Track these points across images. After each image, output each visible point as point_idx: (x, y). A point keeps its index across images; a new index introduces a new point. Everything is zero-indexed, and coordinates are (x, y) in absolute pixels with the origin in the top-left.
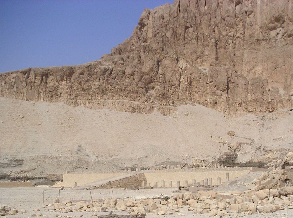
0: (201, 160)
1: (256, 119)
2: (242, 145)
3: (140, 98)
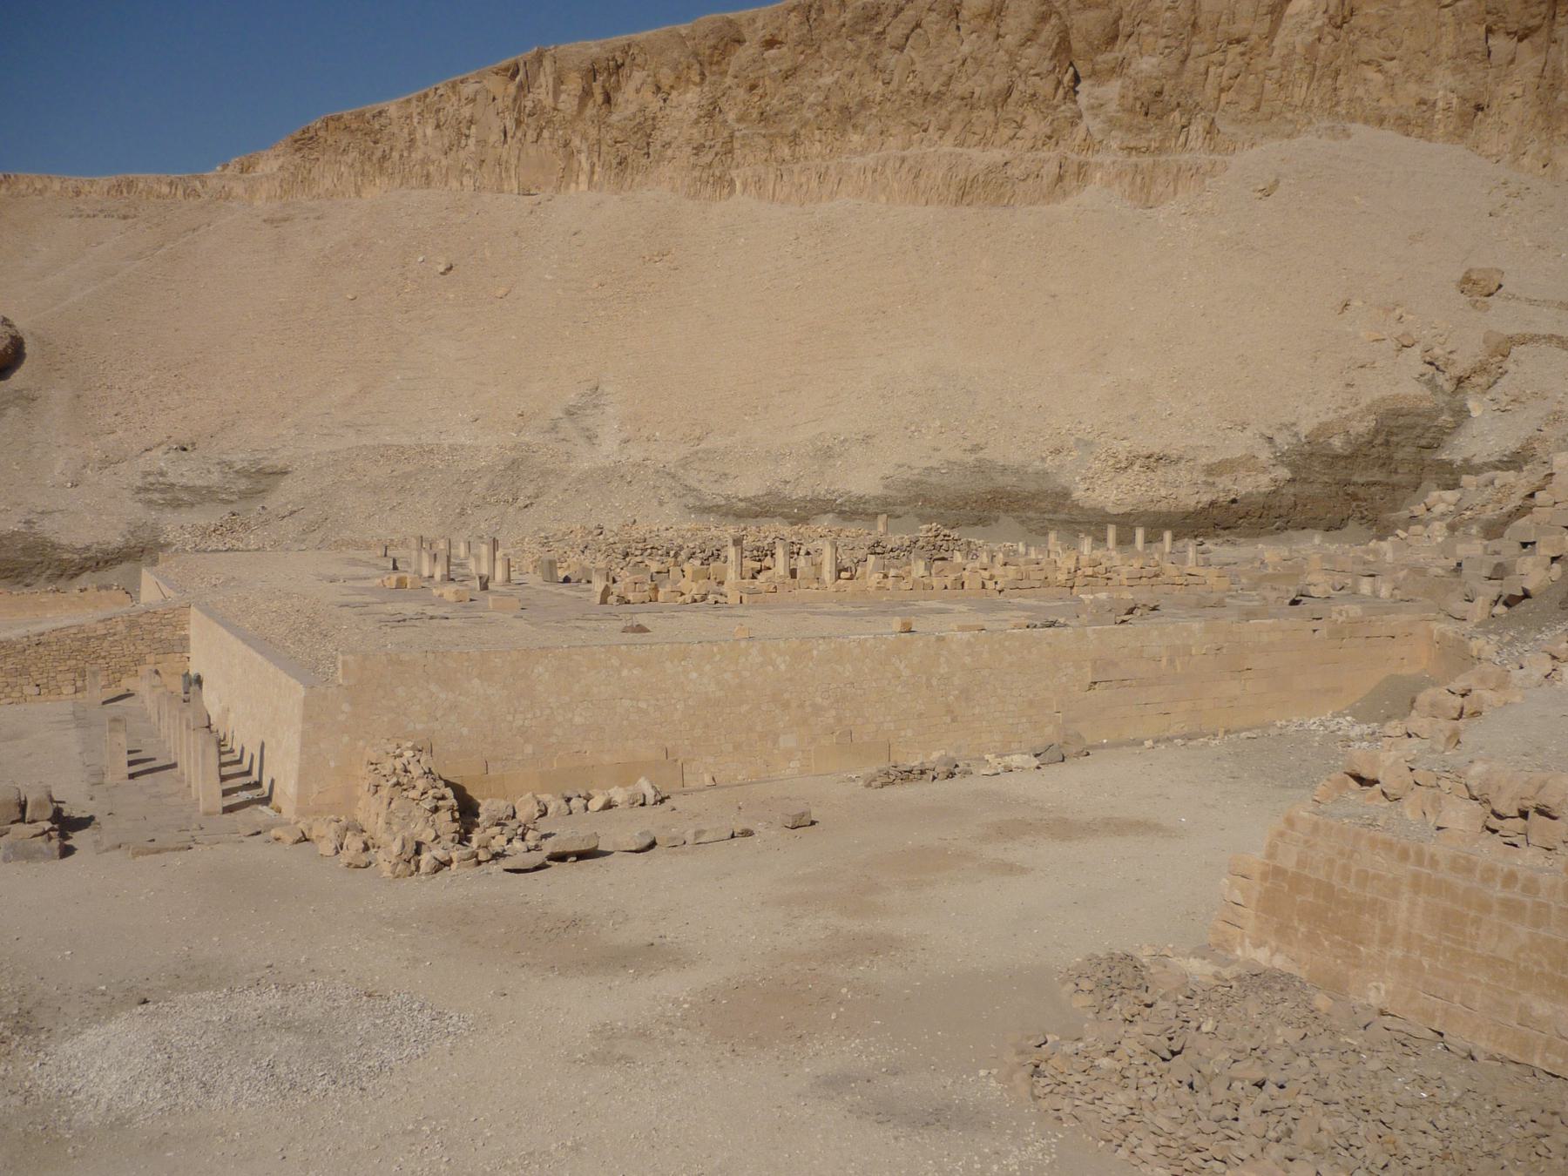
0: (1137, 457)
3: (1020, 127)
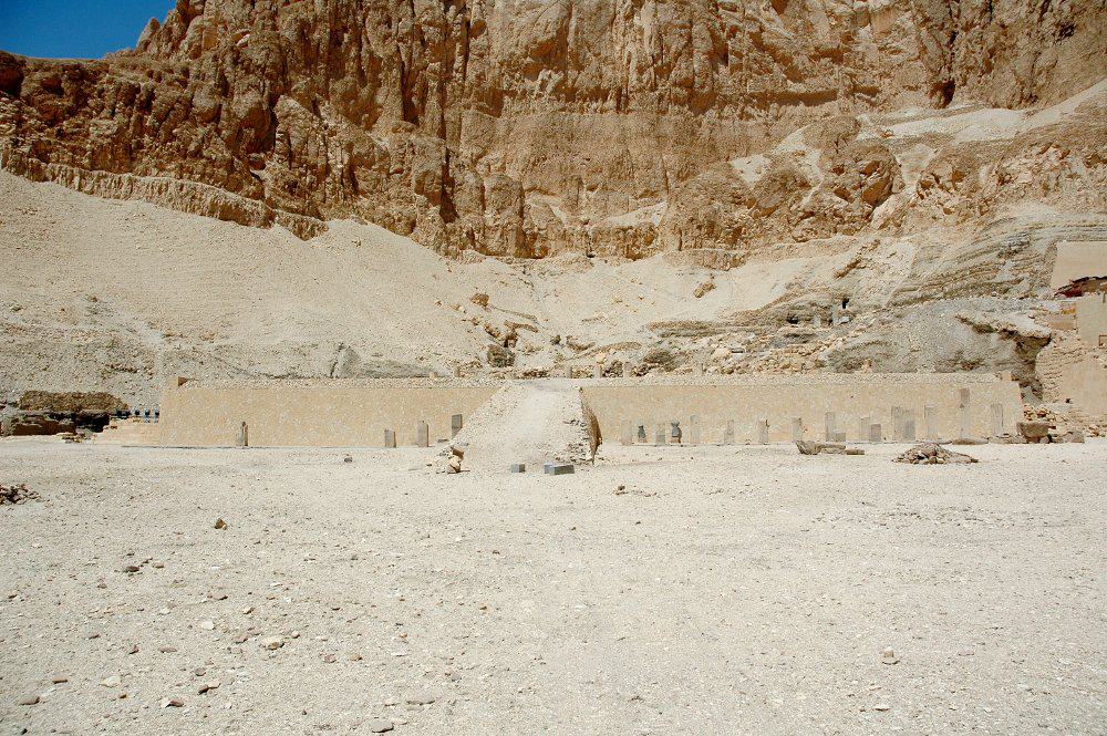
1: (512, 271)
2: (517, 330)
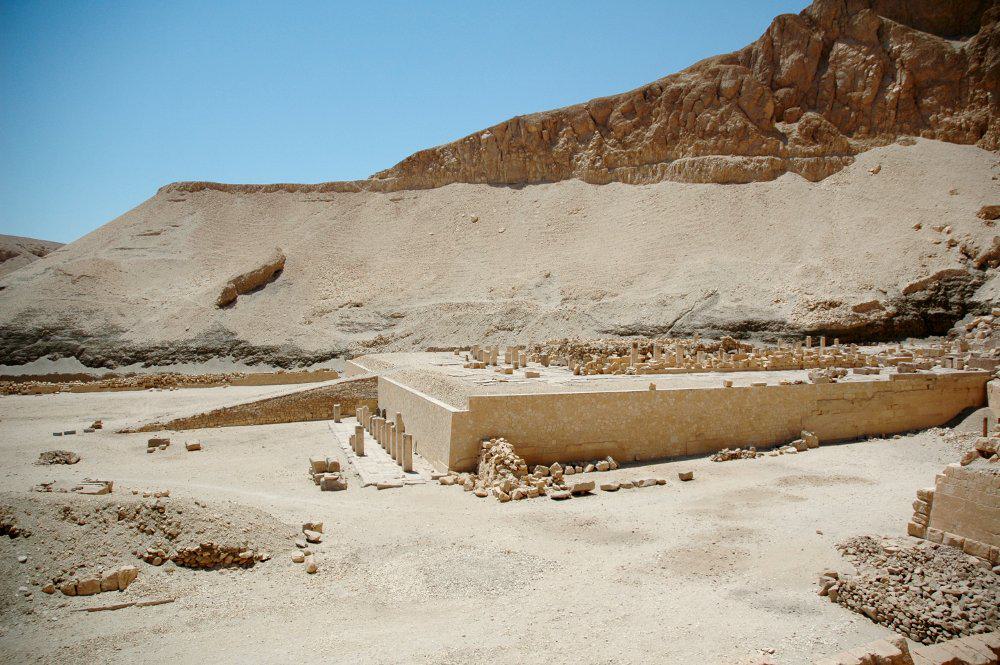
0: (818, 304)
